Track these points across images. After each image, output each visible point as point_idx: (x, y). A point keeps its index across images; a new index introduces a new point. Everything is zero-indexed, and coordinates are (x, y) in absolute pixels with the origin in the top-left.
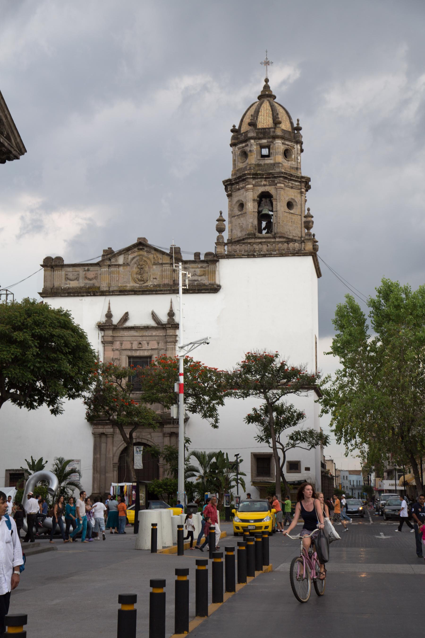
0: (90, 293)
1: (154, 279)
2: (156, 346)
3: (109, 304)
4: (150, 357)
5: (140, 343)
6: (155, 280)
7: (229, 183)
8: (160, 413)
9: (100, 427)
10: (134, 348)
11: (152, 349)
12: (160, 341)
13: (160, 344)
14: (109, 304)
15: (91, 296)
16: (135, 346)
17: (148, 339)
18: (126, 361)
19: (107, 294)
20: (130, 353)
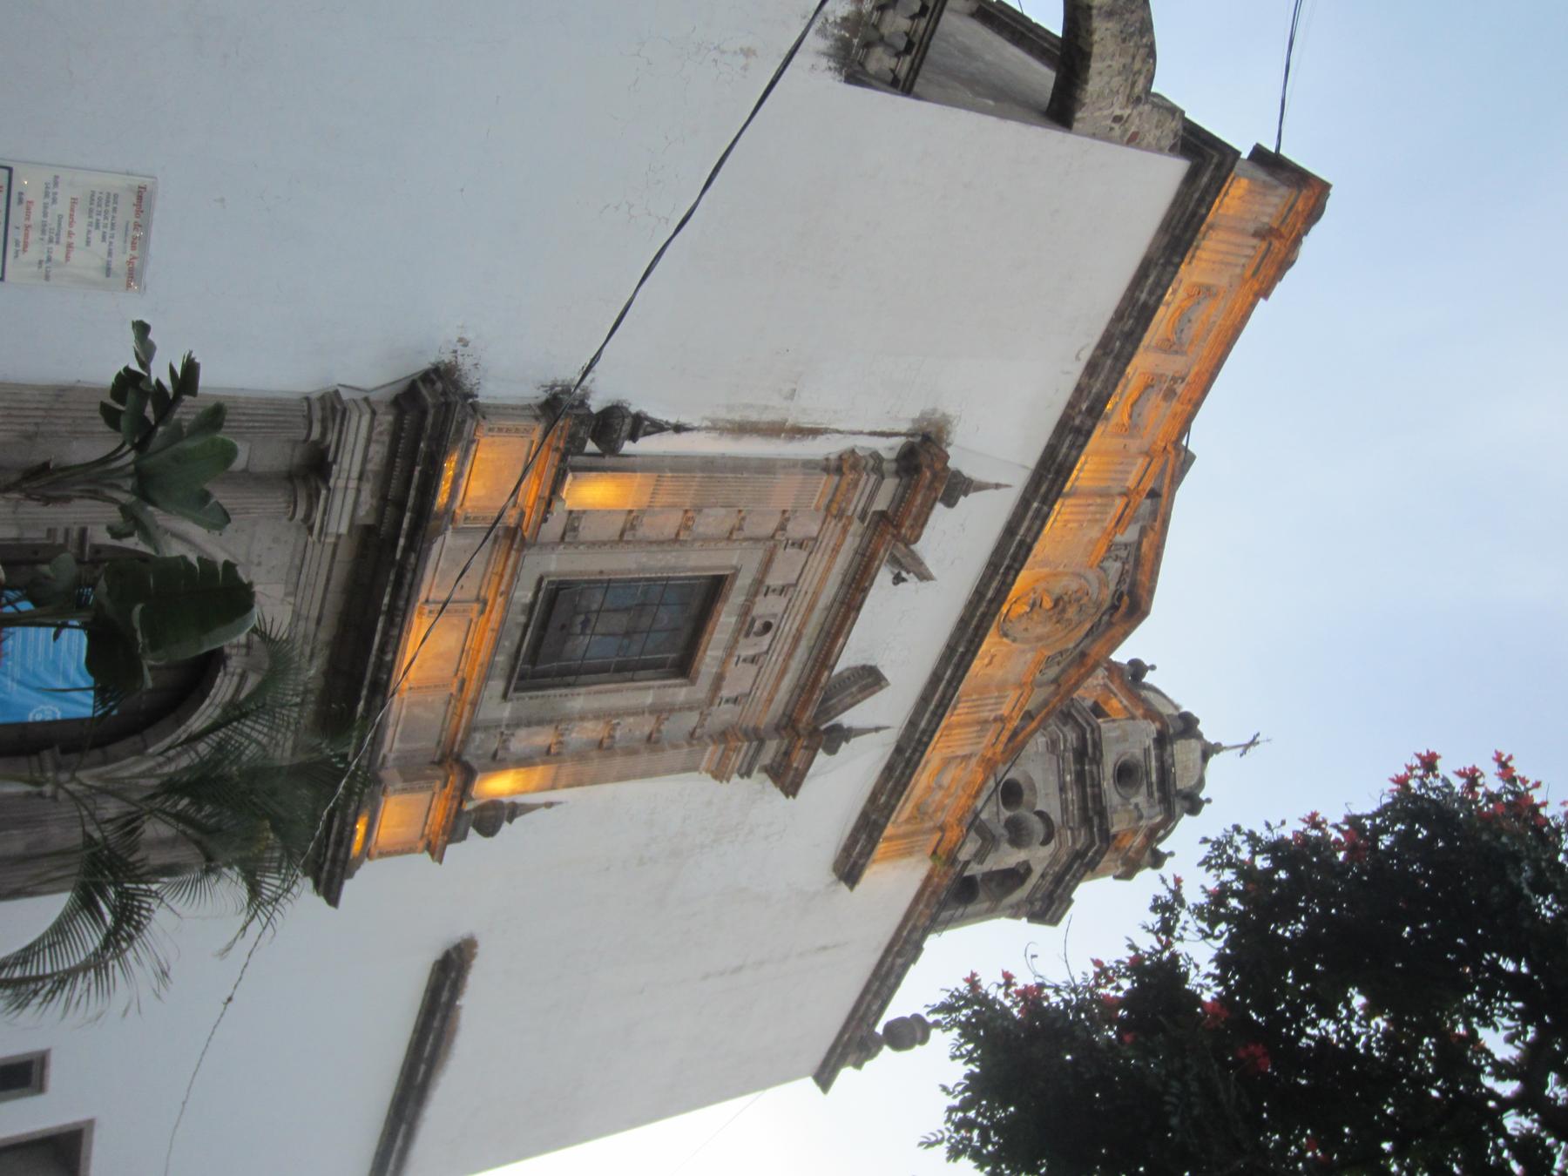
0: (1090, 410)
1: (993, 657)
2: (725, 693)
3: (997, 486)
4: (683, 668)
5: (767, 627)
6: (986, 661)
7: (1090, 750)
8: (385, 750)
9: (378, 452)
10: (760, 598)
11: (719, 680)
12: (738, 709)
13: (730, 705)
14: (997, 486)
15: (1071, 405)
16: (767, 607)
17: (775, 661)
18: (710, 568)
19: (1043, 489)
20: (743, 582)
